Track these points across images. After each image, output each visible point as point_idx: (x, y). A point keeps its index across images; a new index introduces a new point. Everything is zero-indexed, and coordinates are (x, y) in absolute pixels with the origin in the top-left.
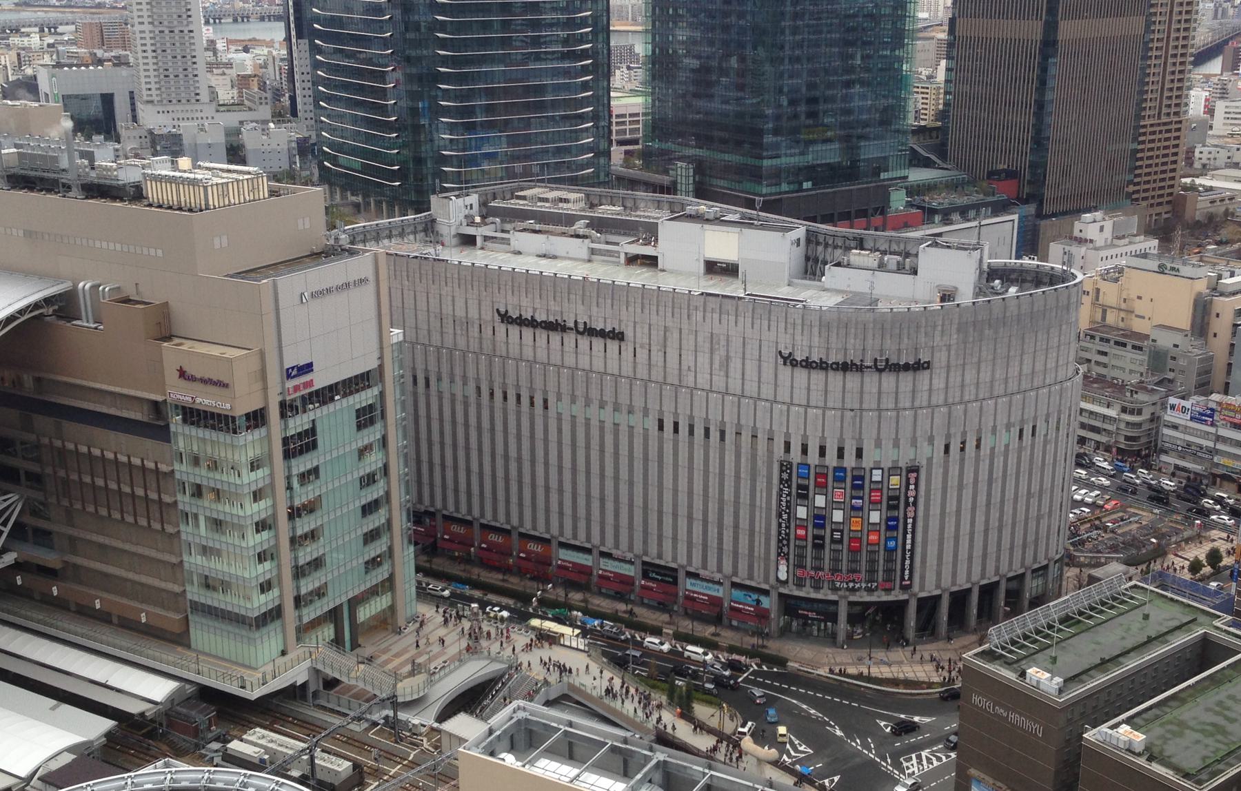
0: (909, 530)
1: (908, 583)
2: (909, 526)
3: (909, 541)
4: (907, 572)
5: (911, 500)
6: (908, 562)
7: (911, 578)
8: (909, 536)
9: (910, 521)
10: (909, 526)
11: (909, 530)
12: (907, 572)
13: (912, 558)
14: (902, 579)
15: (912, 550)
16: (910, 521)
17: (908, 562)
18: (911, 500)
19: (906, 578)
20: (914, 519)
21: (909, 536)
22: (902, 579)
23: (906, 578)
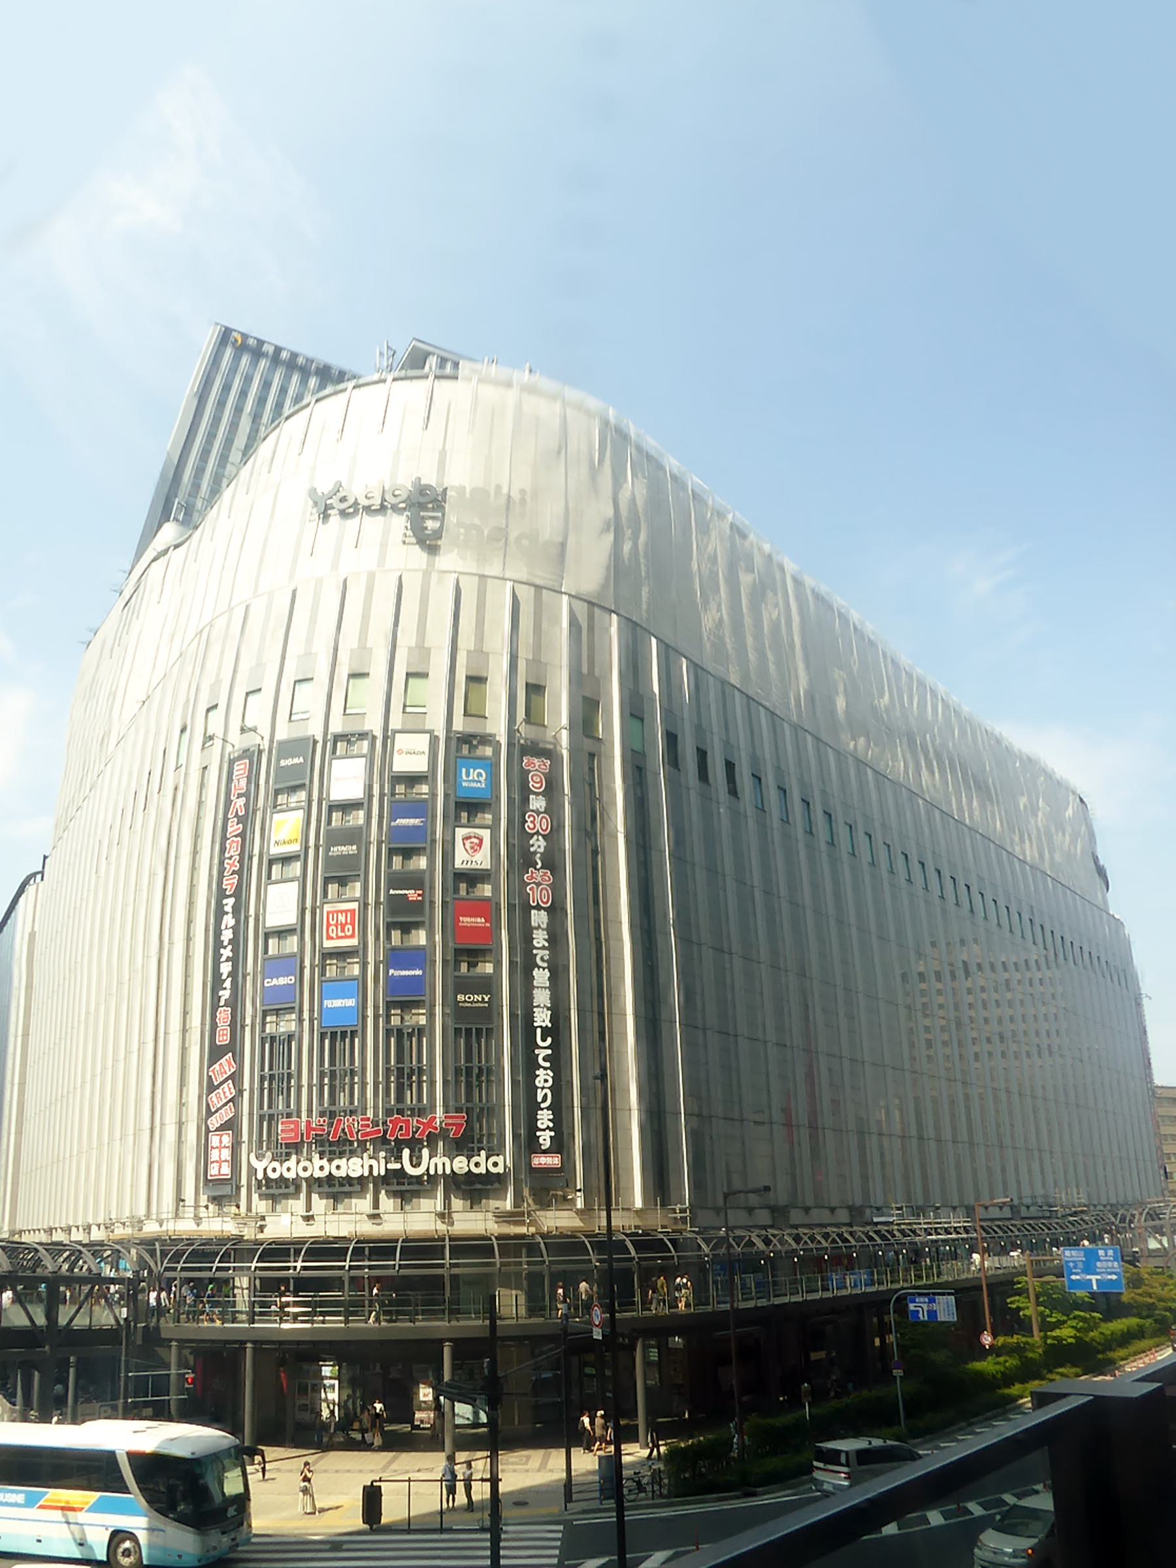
0: (541, 955)
1: (554, 1161)
2: (540, 939)
3: (542, 997)
4: (544, 1118)
5: (538, 845)
6: (544, 1078)
7: (560, 1145)
8: (541, 977)
9: (539, 918)
10: (540, 939)
11: (541, 955)
12: (544, 1118)
13: (558, 1062)
14: (528, 1143)
15: (556, 1031)
16: (539, 918)
17: (544, 1078)
18: (538, 845)
19: (545, 1138)
20: (555, 910)
21: (541, 977)
22: (528, 1143)
23: (545, 1138)
